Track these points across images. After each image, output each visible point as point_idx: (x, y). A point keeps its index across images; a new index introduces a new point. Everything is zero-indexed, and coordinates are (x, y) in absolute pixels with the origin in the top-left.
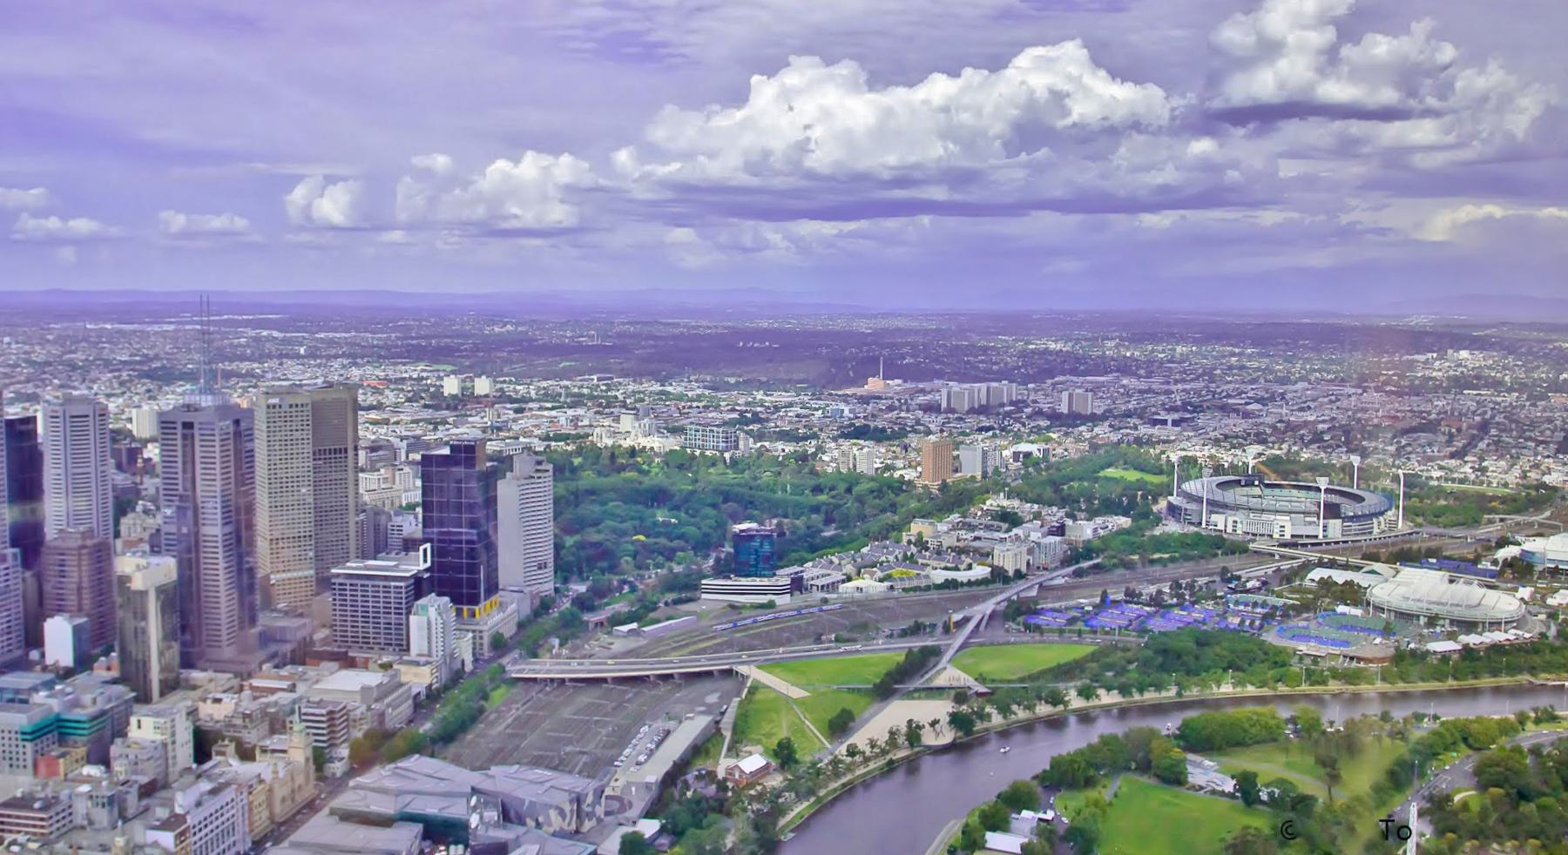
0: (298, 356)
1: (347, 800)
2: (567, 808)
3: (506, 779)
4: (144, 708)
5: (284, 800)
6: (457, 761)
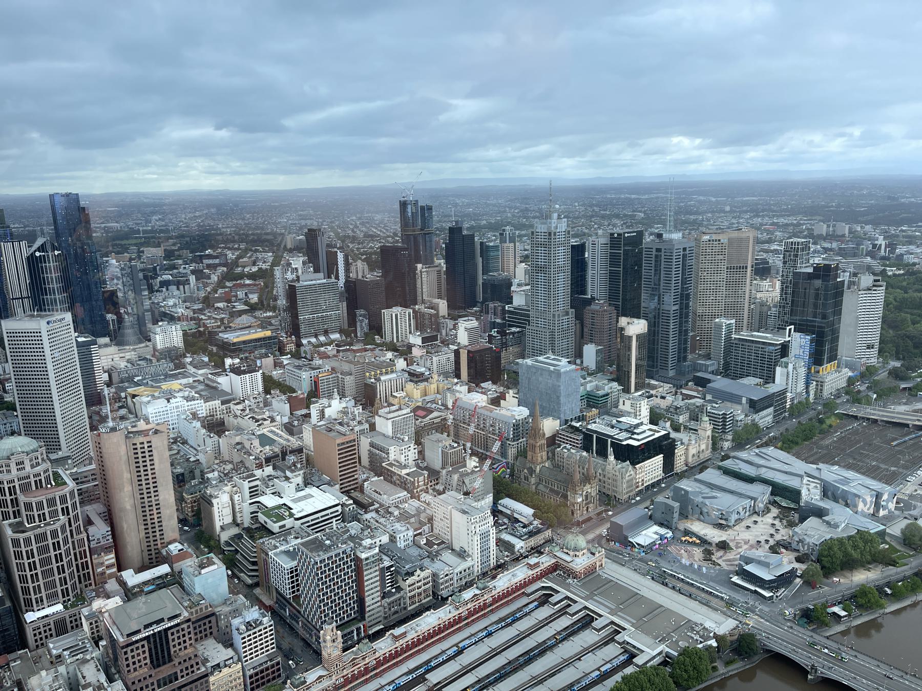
0: (725, 212)
1: (728, 463)
3: (831, 473)
4: (627, 396)
5: (693, 455)
6: (798, 456)
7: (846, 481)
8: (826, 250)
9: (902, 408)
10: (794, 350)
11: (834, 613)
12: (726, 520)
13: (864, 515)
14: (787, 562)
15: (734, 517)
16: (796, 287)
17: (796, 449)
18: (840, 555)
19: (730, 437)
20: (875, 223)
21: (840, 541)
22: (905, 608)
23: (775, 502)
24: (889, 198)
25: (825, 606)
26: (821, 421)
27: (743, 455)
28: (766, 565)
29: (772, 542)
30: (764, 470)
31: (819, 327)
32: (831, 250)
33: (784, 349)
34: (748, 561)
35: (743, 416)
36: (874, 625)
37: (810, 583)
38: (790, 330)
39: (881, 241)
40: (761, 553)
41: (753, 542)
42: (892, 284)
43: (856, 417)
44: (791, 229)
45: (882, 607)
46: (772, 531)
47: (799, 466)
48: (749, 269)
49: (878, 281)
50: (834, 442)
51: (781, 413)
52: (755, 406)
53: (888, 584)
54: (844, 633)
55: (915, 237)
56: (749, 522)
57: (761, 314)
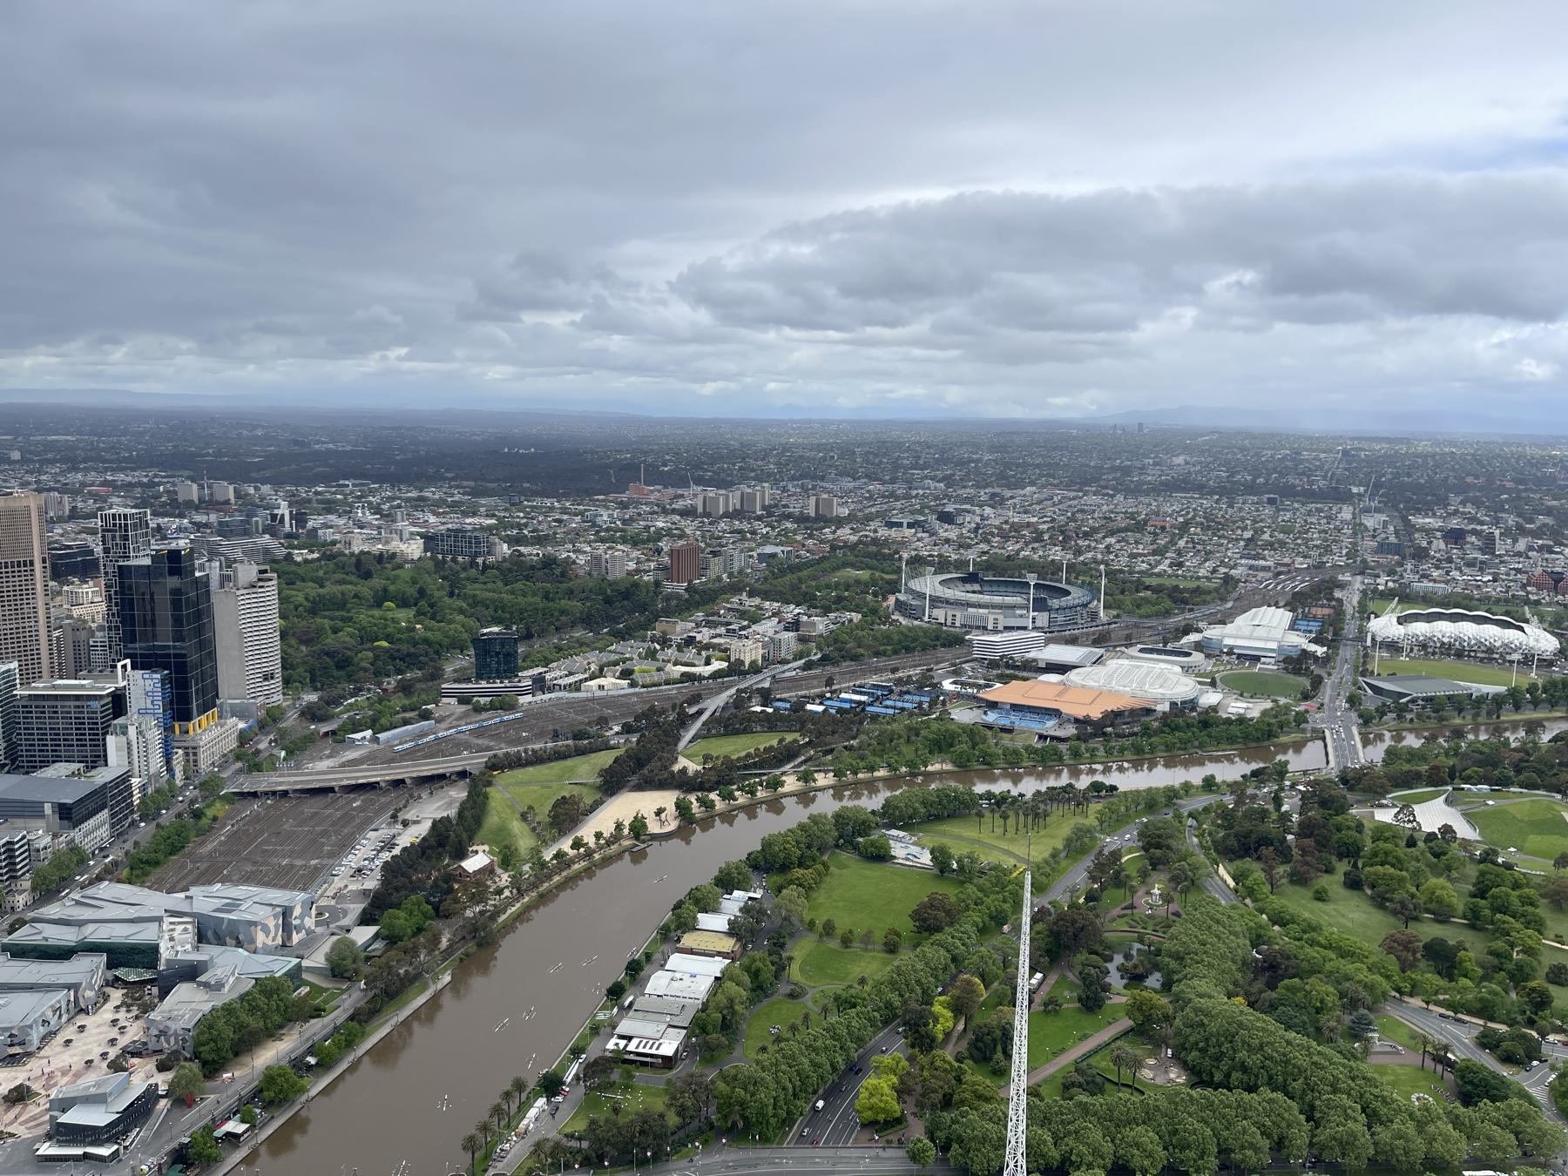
2: (271, 923)
3: (206, 899)
6: (157, 886)
7: (233, 905)
8: (199, 526)
9: (323, 765)
10: (135, 701)
11: (228, 1134)
12: (22, 1044)
13: (267, 951)
14: (143, 1077)
15: (35, 1036)
16: (129, 597)
17: (156, 873)
18: (229, 1033)
19: (27, 884)
20: (277, 482)
21: (228, 1009)
22: (341, 1077)
23: (117, 979)
24: (296, 442)
25: (208, 1129)
26: (197, 815)
27: (53, 910)
28: (94, 1100)
29: (113, 1053)
30: (90, 928)
31: (176, 656)
32: (206, 525)
33: (118, 703)
34: (65, 1105)
35: (49, 839)
36: (297, 1124)
37: (182, 1099)
38: (124, 667)
39: (284, 510)
40: (89, 1081)
41: (78, 1064)
42: (288, 574)
43: (254, 795)
44: (138, 492)
45: (303, 1090)
46: (114, 1033)
47: (154, 901)
48: (38, 566)
49: (265, 571)
50: (221, 844)
51: (126, 817)
52: (70, 815)
53: (311, 1051)
54: (248, 1160)
55: (335, 502)
56: (69, 1032)
57: (76, 645)
